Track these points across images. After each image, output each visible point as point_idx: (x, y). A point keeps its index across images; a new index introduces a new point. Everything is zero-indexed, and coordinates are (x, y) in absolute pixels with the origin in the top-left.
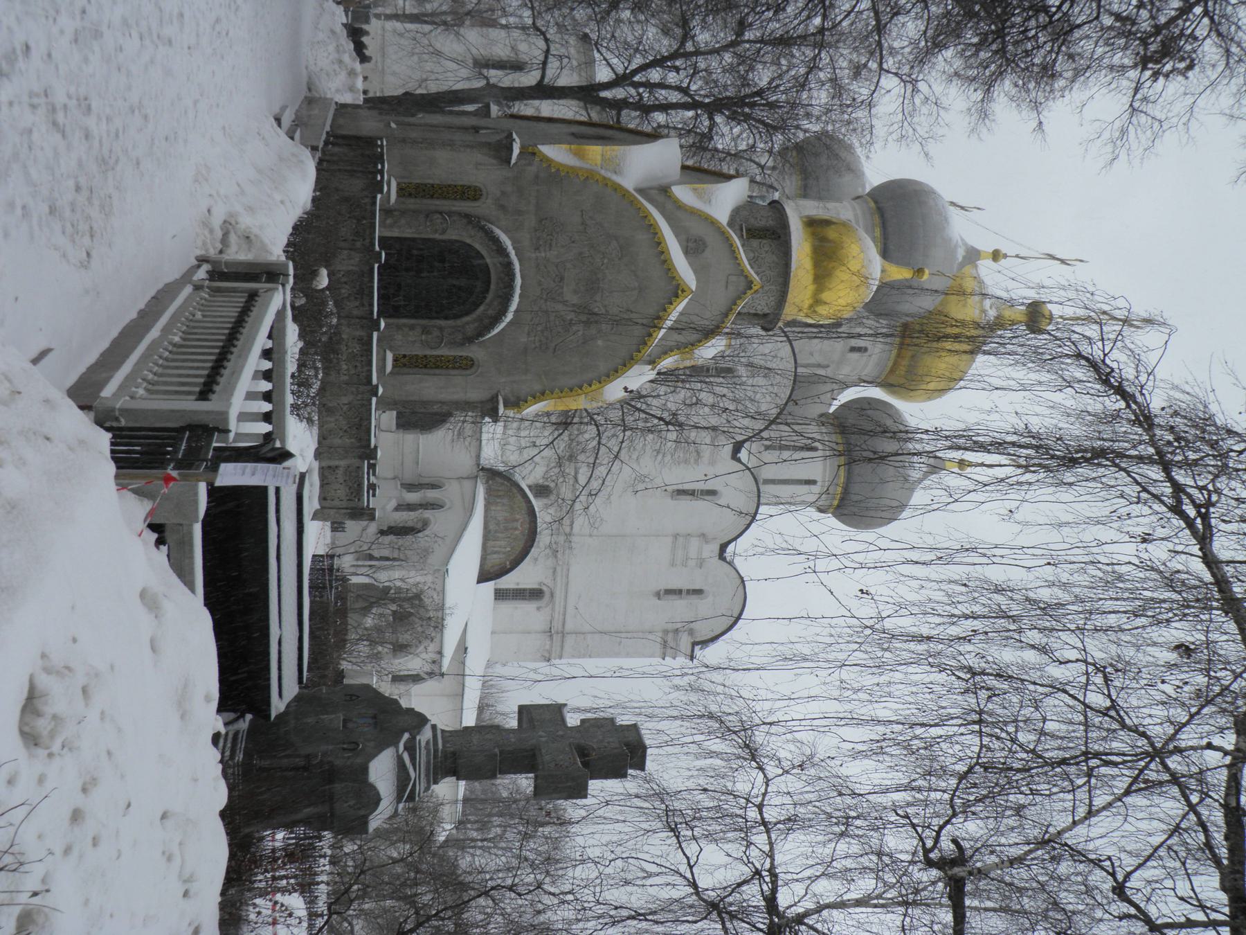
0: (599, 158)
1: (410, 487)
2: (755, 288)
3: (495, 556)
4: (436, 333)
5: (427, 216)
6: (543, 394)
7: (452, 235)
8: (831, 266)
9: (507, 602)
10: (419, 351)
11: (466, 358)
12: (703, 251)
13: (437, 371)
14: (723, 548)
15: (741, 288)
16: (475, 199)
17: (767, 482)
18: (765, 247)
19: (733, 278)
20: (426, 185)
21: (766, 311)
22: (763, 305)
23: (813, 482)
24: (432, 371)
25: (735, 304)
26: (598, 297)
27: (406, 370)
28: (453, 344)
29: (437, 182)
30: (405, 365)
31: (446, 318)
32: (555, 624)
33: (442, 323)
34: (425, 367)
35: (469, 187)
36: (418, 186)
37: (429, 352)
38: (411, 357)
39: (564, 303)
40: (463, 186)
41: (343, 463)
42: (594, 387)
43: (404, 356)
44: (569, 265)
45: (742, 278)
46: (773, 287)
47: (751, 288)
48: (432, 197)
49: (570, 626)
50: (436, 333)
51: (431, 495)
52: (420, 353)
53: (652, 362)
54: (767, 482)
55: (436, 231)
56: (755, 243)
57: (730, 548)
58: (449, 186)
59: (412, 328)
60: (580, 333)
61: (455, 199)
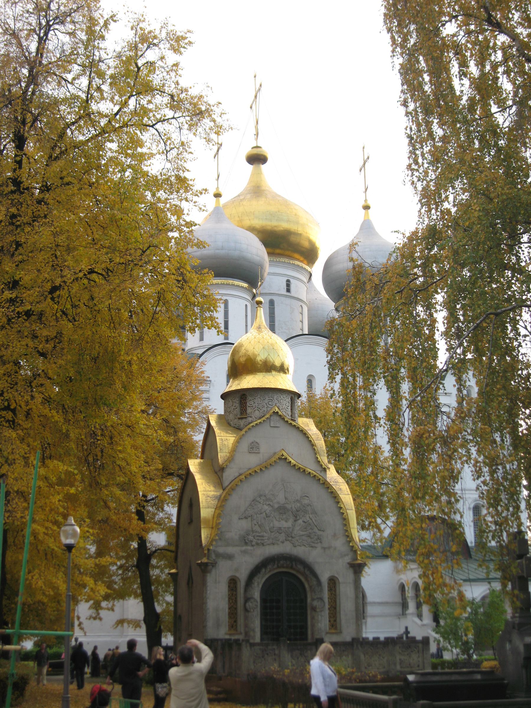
0: (208, 510)
1: (404, 605)
2: (277, 410)
5: (246, 610)
6: (348, 536)
8: (261, 363)
10: (326, 613)
11: (329, 584)
15: (278, 418)
18: (252, 403)
20: (229, 614)
22: (286, 401)
24: (338, 605)
25: (287, 421)
26: (288, 506)
28: (322, 590)
29: (227, 606)
31: (306, 597)
33: (309, 600)
35: (229, 586)
36: (230, 617)
37: (327, 606)
38: (330, 617)
39: (294, 526)
40: (229, 591)
41: (398, 657)
42: (342, 506)
43: (330, 621)
44: (271, 525)
45: (272, 418)
46: (275, 397)
48: (236, 609)
50: (315, 603)
51: (410, 593)
52: (327, 612)
53: (325, 470)
55: (257, 606)
56: (249, 410)
58: (229, 598)
59: (313, 618)
60: (311, 516)
61: (236, 595)
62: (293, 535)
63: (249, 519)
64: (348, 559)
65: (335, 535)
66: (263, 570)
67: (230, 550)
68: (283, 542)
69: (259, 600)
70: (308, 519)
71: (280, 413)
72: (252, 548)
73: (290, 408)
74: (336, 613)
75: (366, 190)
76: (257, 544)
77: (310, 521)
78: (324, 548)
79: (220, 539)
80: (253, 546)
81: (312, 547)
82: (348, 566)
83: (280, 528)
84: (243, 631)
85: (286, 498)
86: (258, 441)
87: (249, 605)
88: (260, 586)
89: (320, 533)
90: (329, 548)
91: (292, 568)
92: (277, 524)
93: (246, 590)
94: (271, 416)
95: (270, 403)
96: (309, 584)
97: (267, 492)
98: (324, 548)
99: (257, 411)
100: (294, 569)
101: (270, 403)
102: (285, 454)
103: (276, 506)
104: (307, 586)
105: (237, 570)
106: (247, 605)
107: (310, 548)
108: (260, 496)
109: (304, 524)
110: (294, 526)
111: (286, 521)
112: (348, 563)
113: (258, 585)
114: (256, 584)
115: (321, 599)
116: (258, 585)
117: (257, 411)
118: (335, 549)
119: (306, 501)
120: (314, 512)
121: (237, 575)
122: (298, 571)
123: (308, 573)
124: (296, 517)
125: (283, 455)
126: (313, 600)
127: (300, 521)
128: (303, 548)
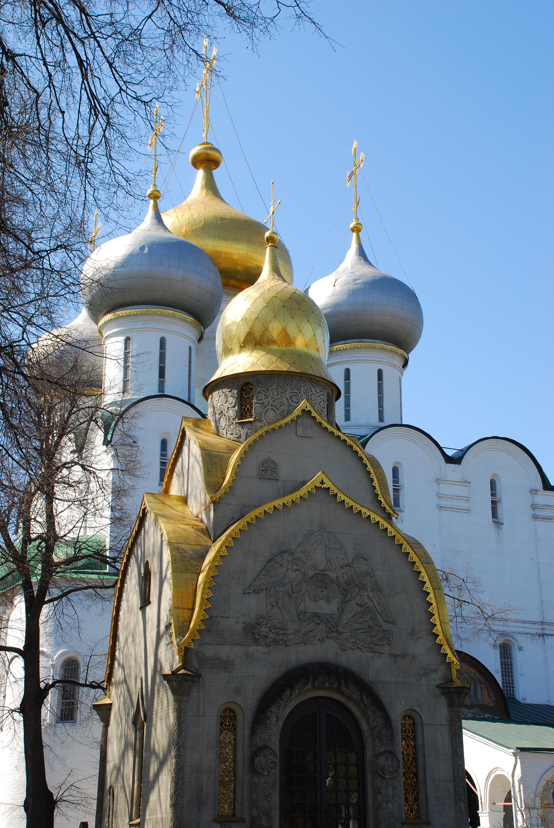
3: (479, 695)
4: (382, 761)
7: (275, 742)
9: (516, 684)
12: (273, 462)
13: (420, 760)
14: (449, 460)
15: (310, 422)
16: (234, 717)
17: (381, 419)
19: (300, 431)
21: (324, 397)
22: (321, 398)
23: (380, 372)
26: (333, 575)
27: (422, 797)
28: (392, 737)
30: (416, 799)
32: (535, 631)
33: (369, 755)
34: (416, 774)
39: (341, 611)
43: (406, 799)
44: (302, 608)
45: (300, 421)
46: (302, 389)
47: (309, 412)
49: (537, 618)
50: (382, 761)
54: (381, 419)
57: (450, 453)
60: (371, 594)
62: (340, 629)
63: (262, 594)
64: (437, 678)
65: (413, 633)
66: (288, 693)
67: (226, 651)
68: (322, 641)
69: (277, 751)
70: (366, 600)
71: (314, 414)
72: (266, 650)
73: (325, 410)
74: (416, 783)
75: (358, 204)
76: (276, 642)
77: (370, 604)
78: (394, 656)
79: (208, 630)
80: (268, 646)
81: (373, 652)
82: (438, 691)
83: (317, 615)
84: (247, 817)
85: (328, 561)
86: (275, 458)
87: (260, 760)
88: (281, 724)
89: (386, 626)
90: (403, 656)
91: (338, 690)
92: (312, 606)
93: (253, 733)
94: (298, 417)
95: (294, 399)
96: (369, 724)
97: (294, 547)
98: (394, 656)
99: (270, 412)
100: (343, 694)
101: (294, 399)
102: (326, 480)
103: (311, 573)
104: (364, 726)
105: (238, 691)
106: (257, 760)
107: (370, 655)
108: (282, 553)
109: (360, 609)
110: (341, 611)
111: (328, 601)
112: (437, 686)
113: (277, 721)
114: (274, 719)
115: (392, 753)
116: (277, 721)
117: (270, 412)
118: (414, 657)
119: (362, 566)
120: (377, 589)
122: (349, 698)
123: (366, 701)
125: (322, 483)
126: (377, 755)
128: (357, 652)
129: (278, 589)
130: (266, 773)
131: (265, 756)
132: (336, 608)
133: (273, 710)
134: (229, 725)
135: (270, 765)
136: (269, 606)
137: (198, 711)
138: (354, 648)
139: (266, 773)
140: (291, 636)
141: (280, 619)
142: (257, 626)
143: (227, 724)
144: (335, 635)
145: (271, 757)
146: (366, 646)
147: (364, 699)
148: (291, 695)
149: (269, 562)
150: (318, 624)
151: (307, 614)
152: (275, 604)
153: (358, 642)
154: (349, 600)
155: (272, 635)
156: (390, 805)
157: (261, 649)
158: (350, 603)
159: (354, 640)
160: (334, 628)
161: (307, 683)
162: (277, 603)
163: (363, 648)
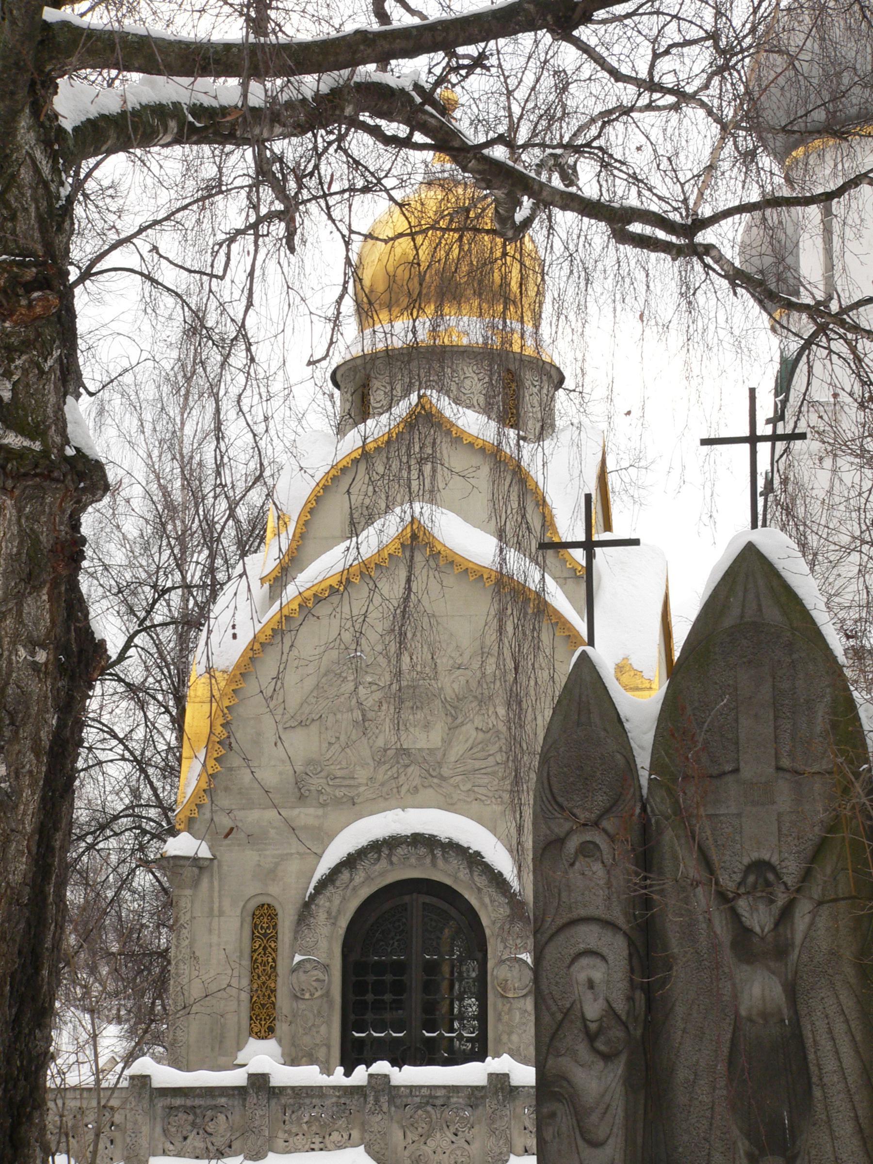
39: (447, 742)
62: (446, 771)
63: (314, 728)
72: (320, 812)
80: (323, 805)
109: (481, 735)
110: (447, 742)
121: (274, 889)
124: (455, 718)
127: (469, 729)
129: (339, 716)
130: (307, 996)
131: (305, 972)
132: (440, 739)
133: (322, 902)
134: (268, 928)
135: (314, 984)
136: (325, 745)
137: (211, 909)
138: (469, 800)
139: (307, 996)
140: (362, 789)
141: (344, 763)
142: (304, 776)
143: (265, 925)
144: (436, 780)
145: (315, 972)
146: (490, 794)
147: (476, 878)
148: (351, 880)
149: (325, 675)
150: (407, 766)
151: (389, 752)
152: (333, 740)
153: (476, 789)
154: (462, 724)
155: (328, 789)
156: (515, 1038)
157: (311, 811)
158: (464, 728)
159: (469, 786)
160: (434, 770)
161: (378, 859)
162: (338, 738)
163: (484, 798)
